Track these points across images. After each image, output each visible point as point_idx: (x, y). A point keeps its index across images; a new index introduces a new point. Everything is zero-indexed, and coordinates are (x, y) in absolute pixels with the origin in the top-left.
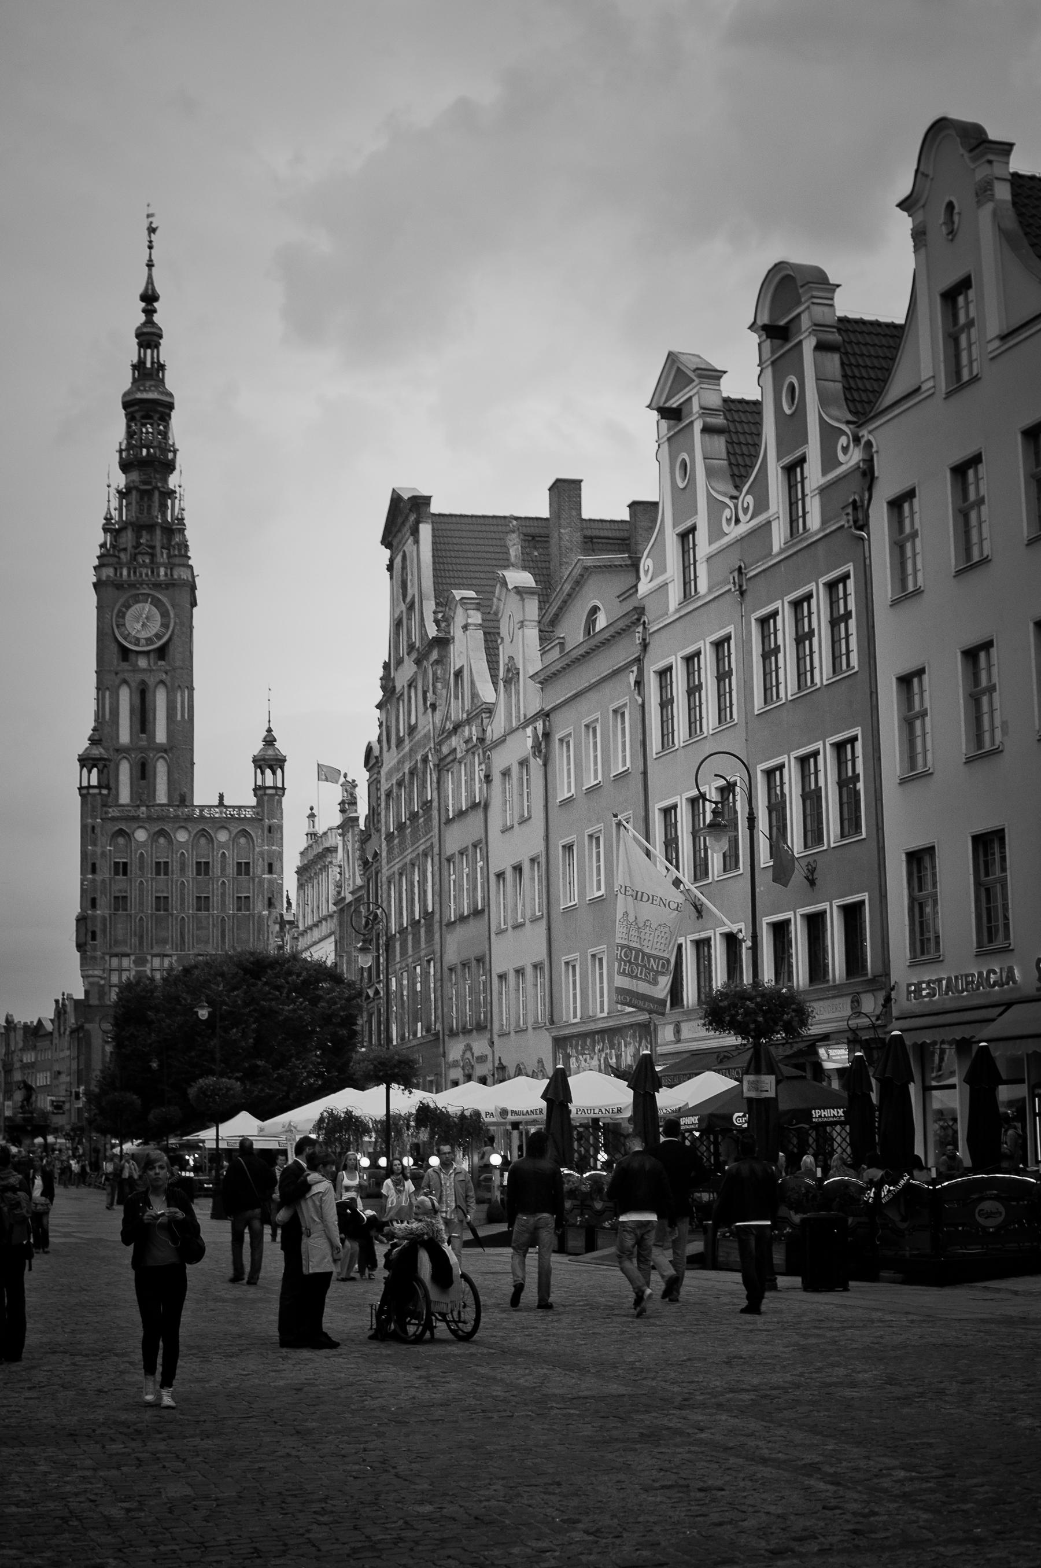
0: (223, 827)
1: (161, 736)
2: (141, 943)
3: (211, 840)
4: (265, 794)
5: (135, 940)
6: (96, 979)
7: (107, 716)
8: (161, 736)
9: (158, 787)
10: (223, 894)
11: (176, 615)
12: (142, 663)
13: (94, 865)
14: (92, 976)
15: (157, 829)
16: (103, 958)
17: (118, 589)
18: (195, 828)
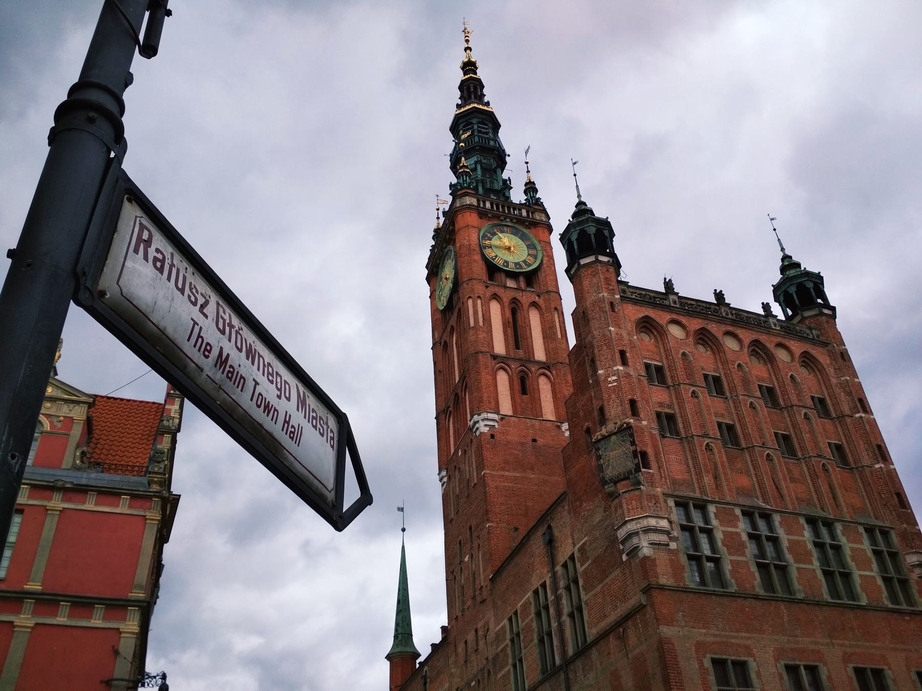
0: (780, 345)
1: (540, 354)
2: (718, 486)
3: (769, 359)
4: (823, 314)
5: (708, 480)
6: (663, 538)
7: (481, 324)
8: (540, 354)
9: (543, 404)
10: (812, 432)
11: (544, 250)
12: (511, 283)
13: (622, 353)
14: (656, 530)
15: (698, 327)
16: (666, 502)
17: (481, 218)
18: (747, 336)
